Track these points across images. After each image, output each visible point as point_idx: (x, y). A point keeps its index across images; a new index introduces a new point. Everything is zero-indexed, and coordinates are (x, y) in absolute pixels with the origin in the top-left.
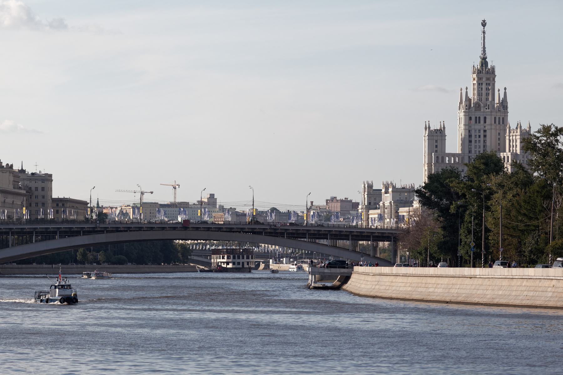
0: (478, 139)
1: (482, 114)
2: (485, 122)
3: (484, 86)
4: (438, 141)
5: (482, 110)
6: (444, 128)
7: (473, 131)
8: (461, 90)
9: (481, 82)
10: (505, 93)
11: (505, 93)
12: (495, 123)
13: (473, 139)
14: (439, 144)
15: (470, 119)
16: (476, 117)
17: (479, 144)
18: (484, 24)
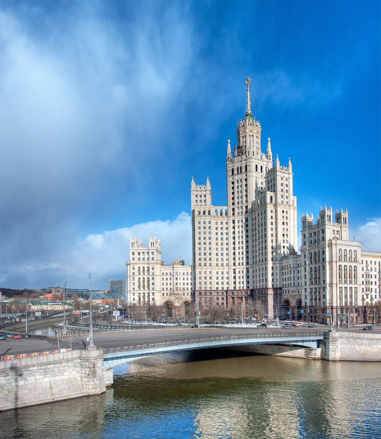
7: (236, 182)
12: (257, 171)
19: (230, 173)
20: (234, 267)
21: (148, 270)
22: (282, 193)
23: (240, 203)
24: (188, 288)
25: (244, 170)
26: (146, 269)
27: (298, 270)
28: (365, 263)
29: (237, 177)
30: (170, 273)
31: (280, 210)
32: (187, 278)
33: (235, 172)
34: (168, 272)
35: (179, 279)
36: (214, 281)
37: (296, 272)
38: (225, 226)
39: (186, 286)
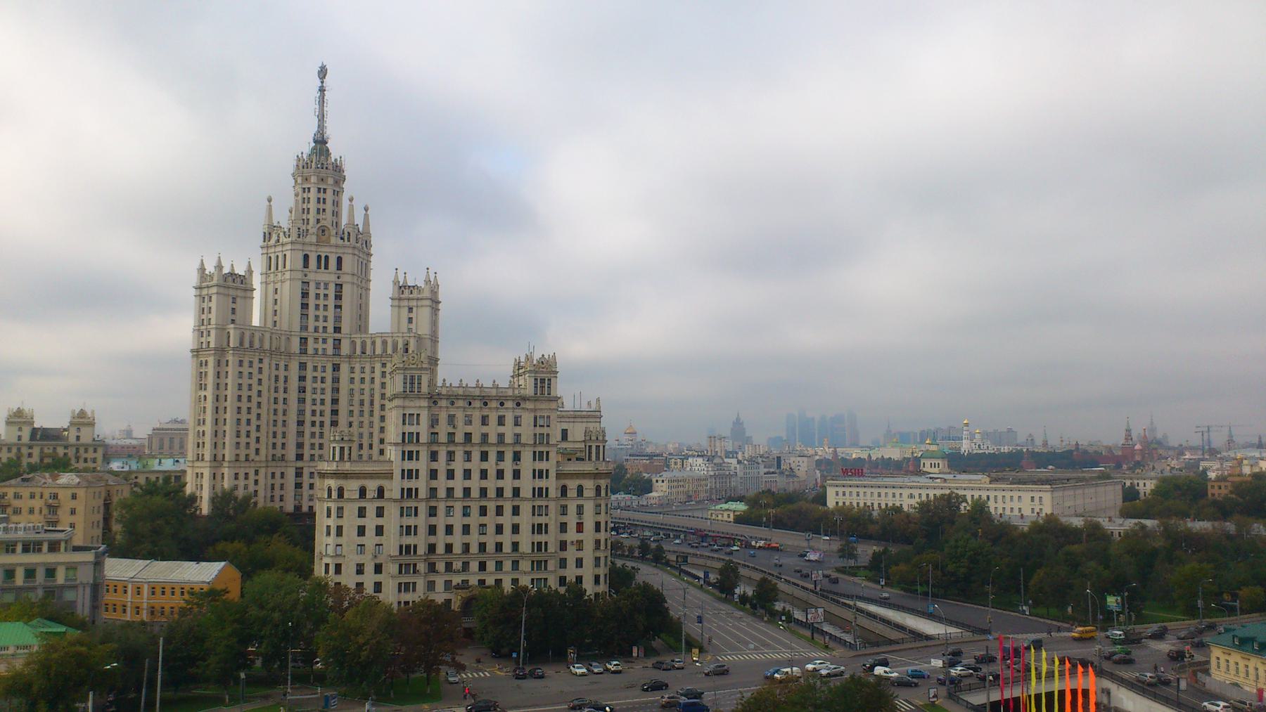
0: (321, 302)
1: (334, 250)
3: (329, 196)
4: (238, 300)
5: (333, 240)
7: (312, 286)
8: (270, 200)
9: (322, 186)
10: (366, 217)
11: (366, 217)
13: (312, 301)
14: (238, 306)
15: (306, 257)
16: (319, 257)
17: (326, 313)
18: (323, 72)
20: (299, 464)
29: (315, 276)
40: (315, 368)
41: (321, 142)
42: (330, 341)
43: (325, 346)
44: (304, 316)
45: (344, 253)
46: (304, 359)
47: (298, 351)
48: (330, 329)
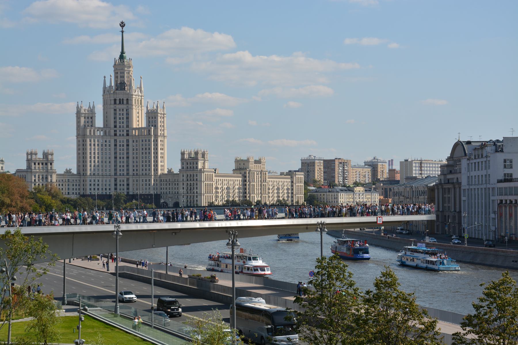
0: (121, 116)
1: (125, 96)
2: (127, 103)
6: (94, 107)
7: (118, 110)
8: (105, 77)
9: (122, 71)
15: (115, 100)
18: (122, 25)
19: (113, 102)
20: (116, 177)
21: (47, 178)
22: (160, 128)
23: (121, 127)
24: (76, 193)
25: (125, 102)
26: (45, 177)
27: (175, 184)
28: (215, 181)
30: (62, 180)
31: (159, 139)
32: (76, 184)
33: (118, 102)
34: (61, 179)
35: (70, 185)
36: (100, 187)
37: (174, 184)
38: (108, 144)
39: (75, 191)
40: (120, 142)
41: (123, 52)
42: (125, 131)
43: (123, 133)
44: (115, 122)
45: (128, 97)
46: (116, 137)
47: (113, 135)
48: (125, 126)
